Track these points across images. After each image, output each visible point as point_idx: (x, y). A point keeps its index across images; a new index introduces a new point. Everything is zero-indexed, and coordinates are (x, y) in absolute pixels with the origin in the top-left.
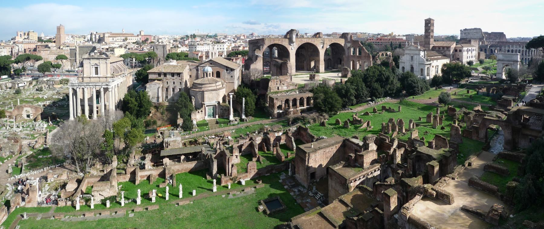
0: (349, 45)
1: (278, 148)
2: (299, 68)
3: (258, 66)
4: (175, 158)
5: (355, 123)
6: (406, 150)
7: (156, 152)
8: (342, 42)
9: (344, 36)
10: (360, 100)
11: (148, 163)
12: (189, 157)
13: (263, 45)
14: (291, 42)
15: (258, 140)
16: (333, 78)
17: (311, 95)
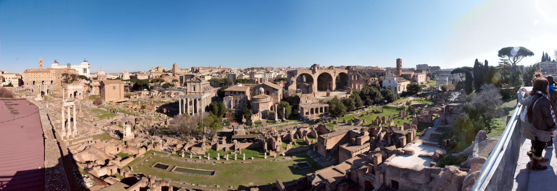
0: (351, 74)
1: (307, 137)
2: (320, 89)
3: (293, 87)
4: (241, 140)
5: (356, 121)
6: (387, 133)
7: (229, 137)
8: (346, 72)
9: (348, 68)
10: (358, 107)
11: (224, 141)
12: (248, 140)
13: (296, 75)
14: (314, 72)
15: (293, 132)
17: (327, 105)
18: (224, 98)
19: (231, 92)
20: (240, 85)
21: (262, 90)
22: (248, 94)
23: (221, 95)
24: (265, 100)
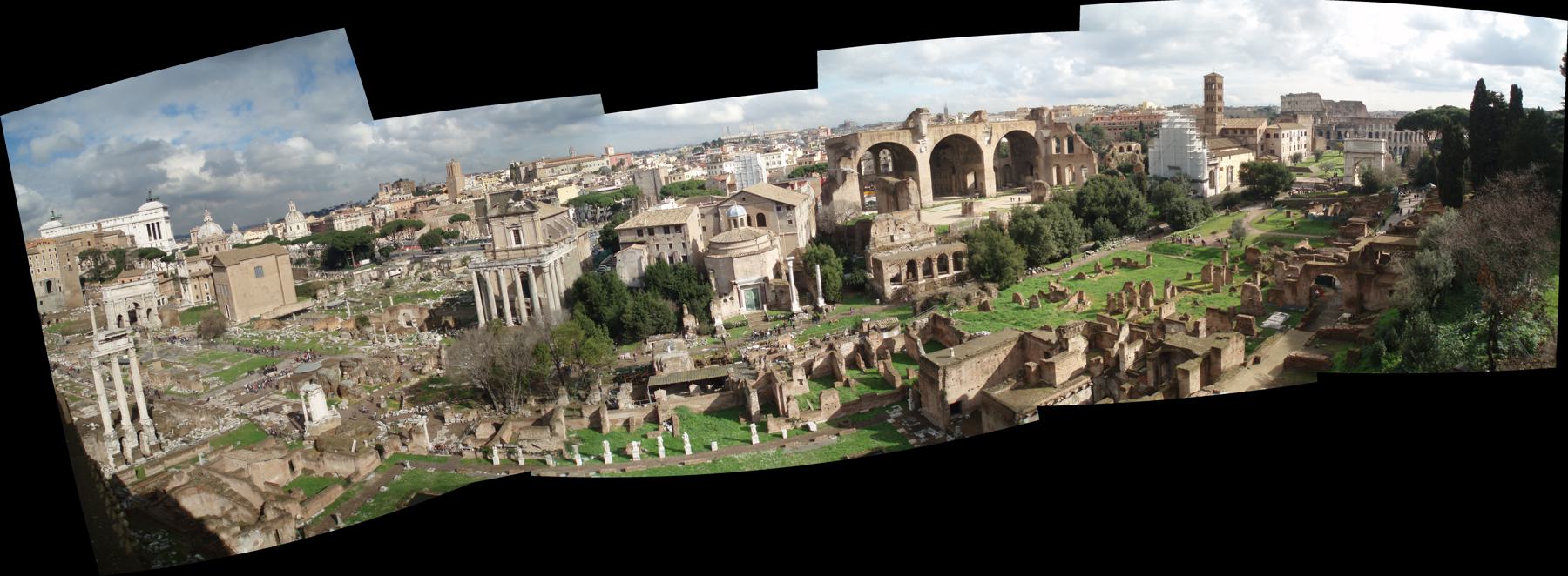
0: (1046, 133)
1: (889, 361)
3: (849, 194)
4: (679, 388)
6: (1146, 343)
7: (641, 381)
8: (1030, 128)
9: (1035, 114)
11: (625, 397)
12: (703, 385)
13: (855, 149)
14: (917, 134)
15: (846, 348)
16: (998, 204)
18: (618, 255)
19: (640, 231)
20: (670, 204)
21: (740, 211)
22: (695, 231)
23: (610, 244)
24: (751, 246)
